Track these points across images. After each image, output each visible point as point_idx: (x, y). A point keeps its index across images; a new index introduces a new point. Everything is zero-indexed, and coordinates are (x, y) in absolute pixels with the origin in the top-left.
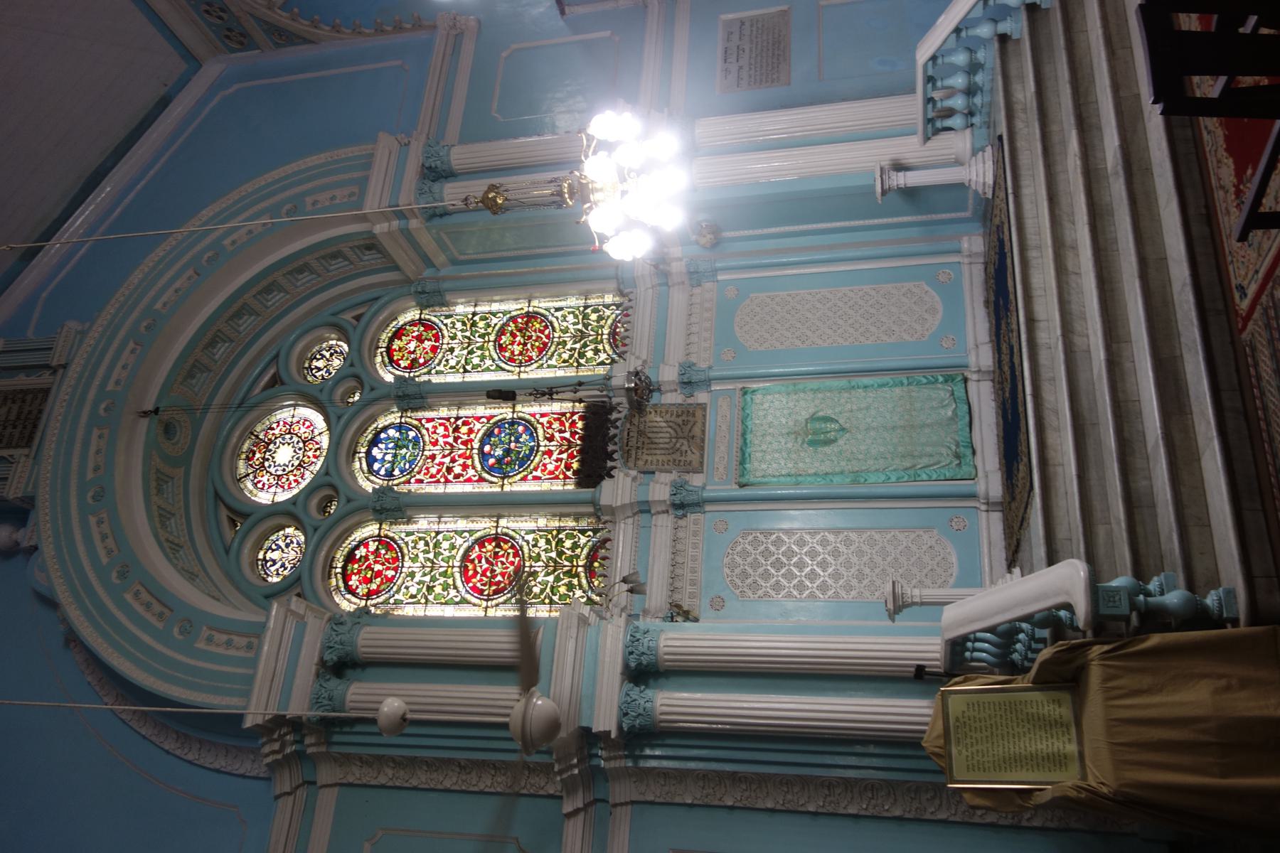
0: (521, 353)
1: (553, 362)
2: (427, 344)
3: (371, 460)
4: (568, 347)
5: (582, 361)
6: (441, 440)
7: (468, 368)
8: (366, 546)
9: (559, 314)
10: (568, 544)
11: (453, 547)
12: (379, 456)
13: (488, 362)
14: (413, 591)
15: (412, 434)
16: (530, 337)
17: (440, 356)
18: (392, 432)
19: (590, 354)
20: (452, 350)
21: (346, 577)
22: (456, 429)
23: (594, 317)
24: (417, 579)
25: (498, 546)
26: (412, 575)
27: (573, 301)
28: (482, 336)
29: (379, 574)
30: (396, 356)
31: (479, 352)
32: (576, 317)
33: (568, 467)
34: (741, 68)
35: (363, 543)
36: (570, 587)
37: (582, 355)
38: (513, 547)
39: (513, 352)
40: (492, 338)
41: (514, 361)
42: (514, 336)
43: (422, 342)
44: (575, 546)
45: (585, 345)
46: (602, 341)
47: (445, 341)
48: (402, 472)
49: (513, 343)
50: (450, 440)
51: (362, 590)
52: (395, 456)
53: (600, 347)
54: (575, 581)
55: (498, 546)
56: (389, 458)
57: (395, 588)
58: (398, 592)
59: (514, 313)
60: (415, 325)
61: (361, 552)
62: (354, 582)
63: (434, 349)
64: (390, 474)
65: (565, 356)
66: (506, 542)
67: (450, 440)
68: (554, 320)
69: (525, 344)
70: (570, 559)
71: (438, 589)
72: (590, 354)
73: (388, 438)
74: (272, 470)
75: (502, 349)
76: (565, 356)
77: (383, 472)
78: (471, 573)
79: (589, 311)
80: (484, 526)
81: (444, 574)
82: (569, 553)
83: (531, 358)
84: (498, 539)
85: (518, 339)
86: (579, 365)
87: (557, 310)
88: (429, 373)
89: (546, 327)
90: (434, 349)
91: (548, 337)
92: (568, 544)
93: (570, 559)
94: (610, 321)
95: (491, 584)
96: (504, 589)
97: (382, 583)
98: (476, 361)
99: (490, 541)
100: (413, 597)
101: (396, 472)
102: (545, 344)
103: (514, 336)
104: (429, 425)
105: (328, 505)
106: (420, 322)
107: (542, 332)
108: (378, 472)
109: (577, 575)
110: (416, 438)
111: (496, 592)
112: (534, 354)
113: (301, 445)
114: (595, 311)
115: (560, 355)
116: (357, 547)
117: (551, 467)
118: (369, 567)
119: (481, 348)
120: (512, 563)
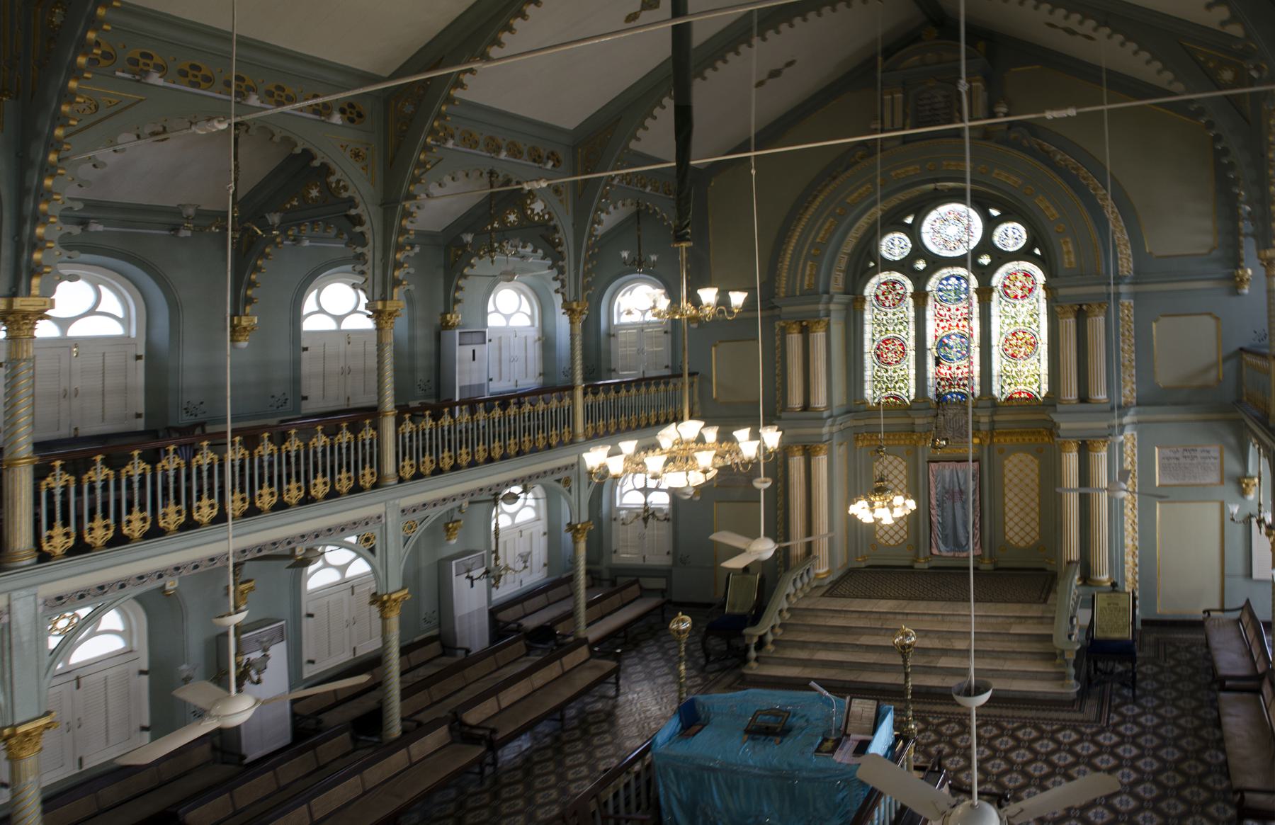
1: (1005, 362)
2: (1020, 293)
3: (947, 279)
15: (963, 296)
18: (964, 285)
21: (885, 283)
51: (879, 293)
61: (898, 286)
62: (884, 287)
63: (1016, 297)
64: (940, 290)
80: (911, 344)
84: (904, 353)
105: (921, 265)
112: (1010, 352)
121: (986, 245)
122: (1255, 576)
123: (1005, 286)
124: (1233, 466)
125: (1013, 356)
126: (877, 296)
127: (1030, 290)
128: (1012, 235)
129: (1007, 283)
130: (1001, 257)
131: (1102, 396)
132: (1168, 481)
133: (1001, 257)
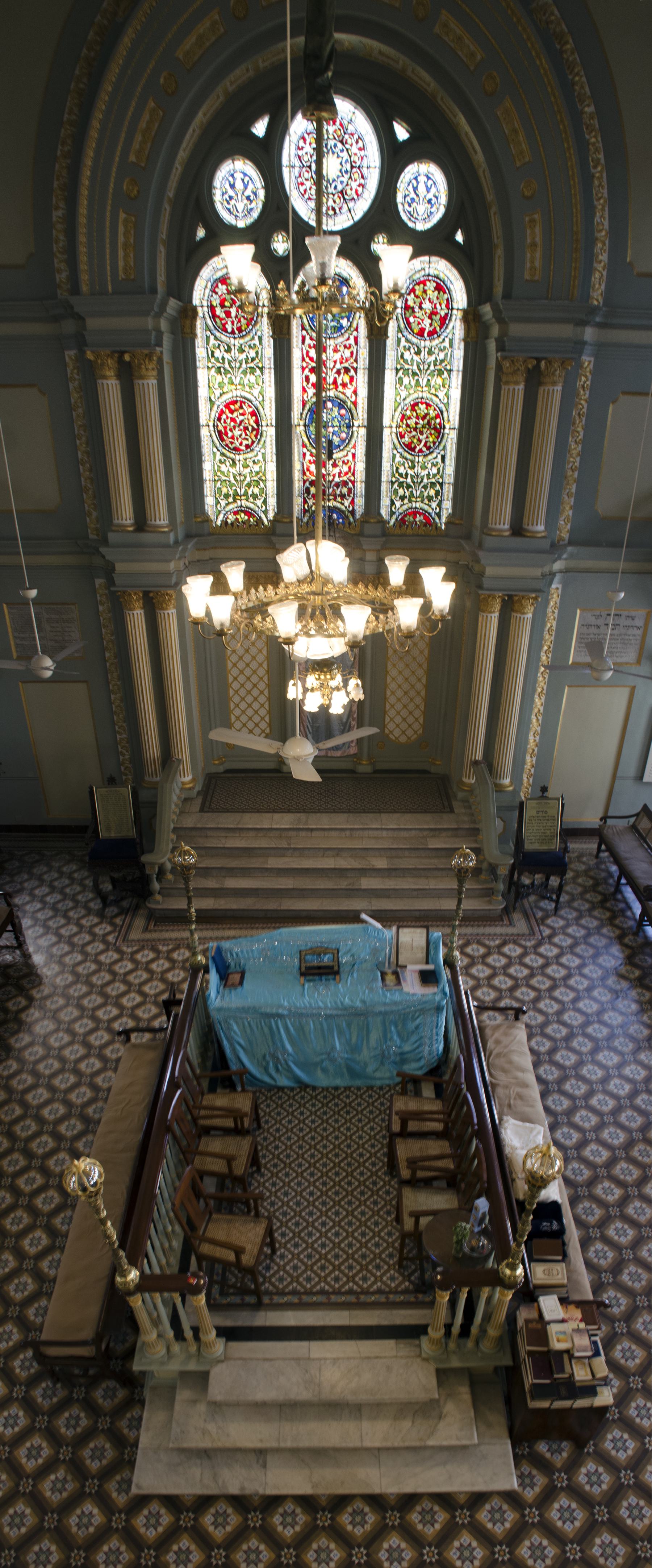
0: (408, 425)
1: (398, 459)
25: (253, 429)
27: (450, 470)
29: (228, 314)
37: (401, 485)
38: (253, 442)
39: (409, 418)
40: (425, 395)
42: (424, 418)
49: (417, 417)
53: (406, 501)
54: (231, 500)
57: (218, 334)
59: (445, 414)
66: (256, 436)
68: (434, 455)
69: (415, 429)
70: (246, 494)
72: (401, 492)
75: (414, 407)
78: (232, 407)
83: (402, 436)
85: (421, 422)
89: (428, 448)
91: (421, 451)
93: (246, 494)
95: (225, 428)
96: (222, 440)
97: (221, 319)
99: (257, 422)
102: (413, 450)
107: (425, 445)
109: (235, 501)
111: (220, 432)
112: (406, 439)
120: (241, 444)
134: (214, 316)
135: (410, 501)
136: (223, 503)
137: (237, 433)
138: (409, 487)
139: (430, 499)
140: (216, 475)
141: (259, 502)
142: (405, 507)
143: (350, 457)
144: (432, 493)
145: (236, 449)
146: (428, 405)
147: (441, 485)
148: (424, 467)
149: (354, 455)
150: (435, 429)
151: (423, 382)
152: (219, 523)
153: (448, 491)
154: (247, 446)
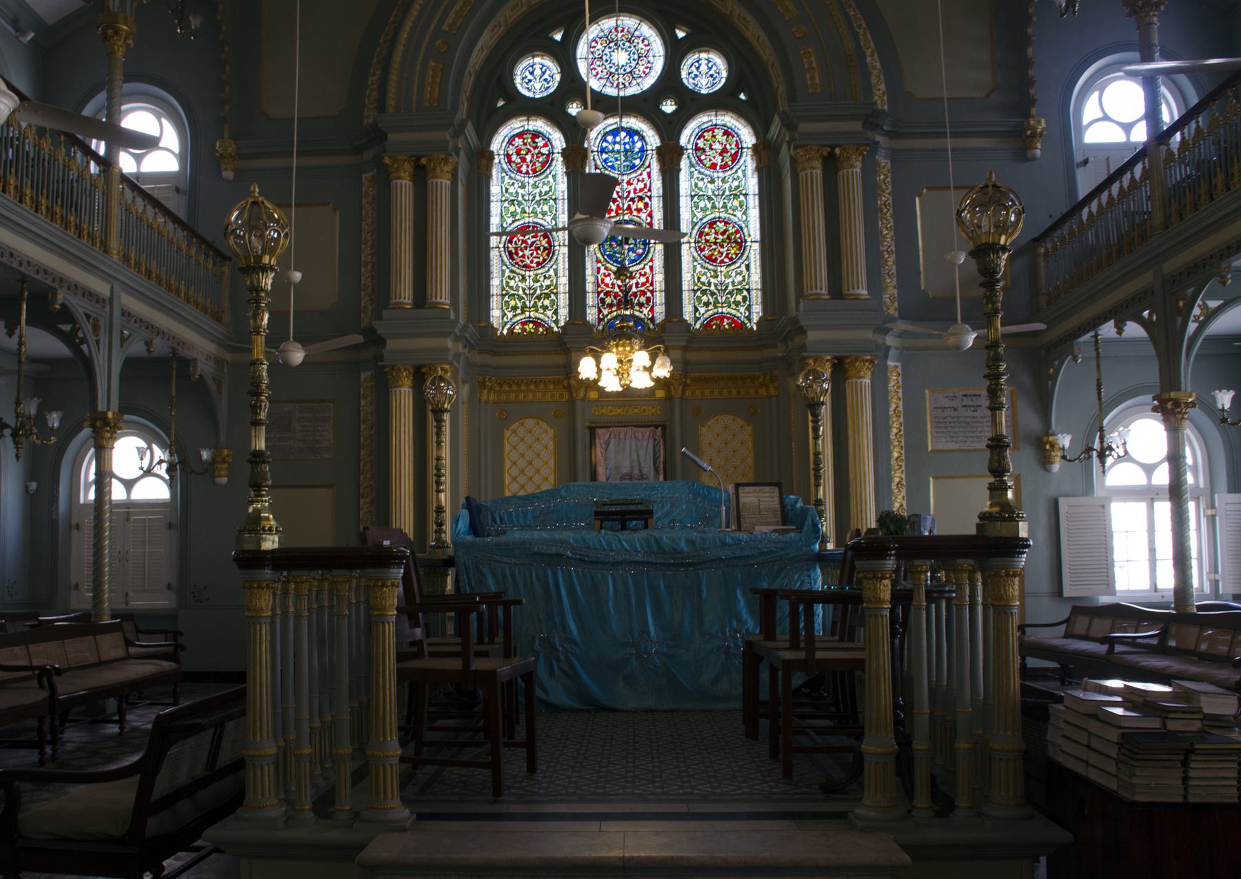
0: (707, 241)
1: (699, 269)
2: (718, 160)
3: (615, 133)
4: (712, 280)
5: (698, 293)
6: (631, 188)
7: (696, 199)
8: (545, 145)
9: (743, 267)
10: (547, 302)
11: (544, 214)
12: (618, 139)
13: (700, 216)
14: (511, 190)
15: (637, 162)
16: (722, 246)
17: (708, 173)
19: (705, 299)
20: (712, 182)
21: (520, 135)
22: (641, 199)
23: (739, 298)
24: (520, 191)
25: (545, 249)
26: (523, 186)
27: (756, 278)
28: (724, 206)
29: (524, 160)
30: (708, 135)
31: (709, 206)
32: (740, 283)
33: (608, 294)
34: (956, 409)
35: (548, 142)
36: (515, 308)
37: (704, 292)
38: (544, 260)
39: (708, 234)
40: (723, 215)
41: (700, 236)
43: (721, 154)
44: (545, 308)
45: (712, 294)
46: (716, 307)
47: (721, 175)
48: (605, 161)
49: (716, 233)
50: (632, 195)
51: (512, 150)
52: (619, 152)
54: (519, 311)
55: (545, 249)
56: (617, 147)
58: (511, 178)
60: (737, 145)
62: (518, 141)
63: (714, 166)
65: (704, 279)
67: (632, 195)
69: (715, 243)
70: (535, 305)
71: (512, 209)
72: (705, 299)
73: (634, 143)
74: (607, 50)
75: (712, 224)
76: (704, 279)
77: (605, 144)
79: (745, 293)
81: (524, 211)
82: (540, 304)
83: (702, 250)
84: (550, 250)
86: (695, 291)
87: (748, 267)
88: (692, 165)
89: (731, 259)
90: (714, 166)
91: (722, 262)
92: (547, 302)
93: (535, 305)
94: (734, 312)
95: (516, 249)
96: (513, 259)
98: (702, 204)
99: (549, 242)
100: (507, 190)
101: (604, 156)
102: (715, 261)
103: (723, 234)
104: (645, 175)
106: (739, 147)
107: (727, 256)
108: (605, 140)
109: (523, 312)
110: (634, 166)
111: (510, 253)
112: (706, 252)
113: (629, 70)
114: (744, 299)
115: (705, 274)
116: (544, 137)
117: (607, 280)
118: (529, 151)
119: (714, 207)
121: (670, 83)
122: (1066, 594)
123: (697, 149)
124: (1030, 421)
125: (711, 259)
126: (508, 156)
127: (734, 157)
128: (707, 70)
129: (701, 143)
130: (692, 103)
131: (864, 292)
132: (940, 446)
133: (692, 103)
134: (510, 162)
135: (716, 307)
136: (510, 315)
137: (527, 252)
138: (712, 294)
139: (737, 304)
140: (503, 289)
141: (549, 313)
142: (710, 313)
143: (647, 269)
144: (739, 298)
145: (526, 266)
146: (726, 223)
147: (748, 290)
148: (727, 276)
149: (651, 268)
150: (735, 242)
151: (719, 204)
152: (505, 332)
153: (756, 297)
154: (538, 264)
